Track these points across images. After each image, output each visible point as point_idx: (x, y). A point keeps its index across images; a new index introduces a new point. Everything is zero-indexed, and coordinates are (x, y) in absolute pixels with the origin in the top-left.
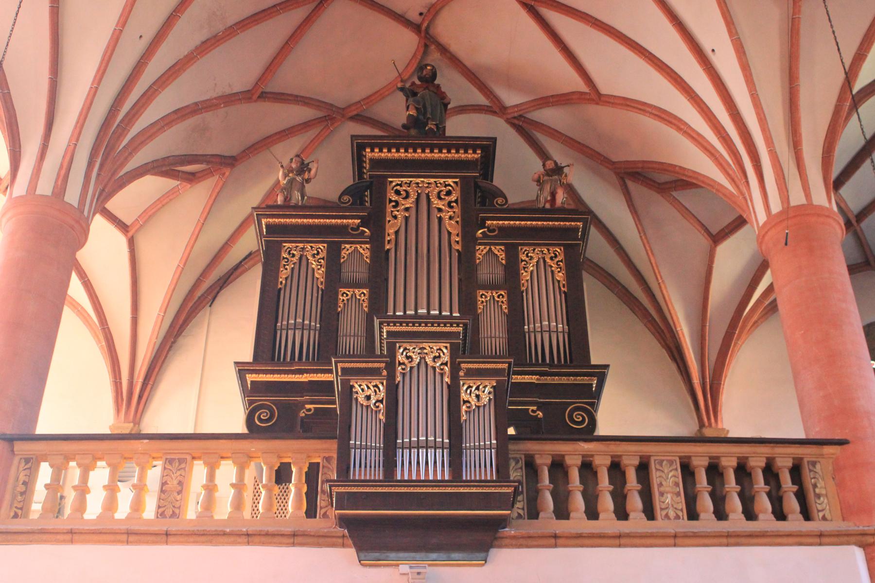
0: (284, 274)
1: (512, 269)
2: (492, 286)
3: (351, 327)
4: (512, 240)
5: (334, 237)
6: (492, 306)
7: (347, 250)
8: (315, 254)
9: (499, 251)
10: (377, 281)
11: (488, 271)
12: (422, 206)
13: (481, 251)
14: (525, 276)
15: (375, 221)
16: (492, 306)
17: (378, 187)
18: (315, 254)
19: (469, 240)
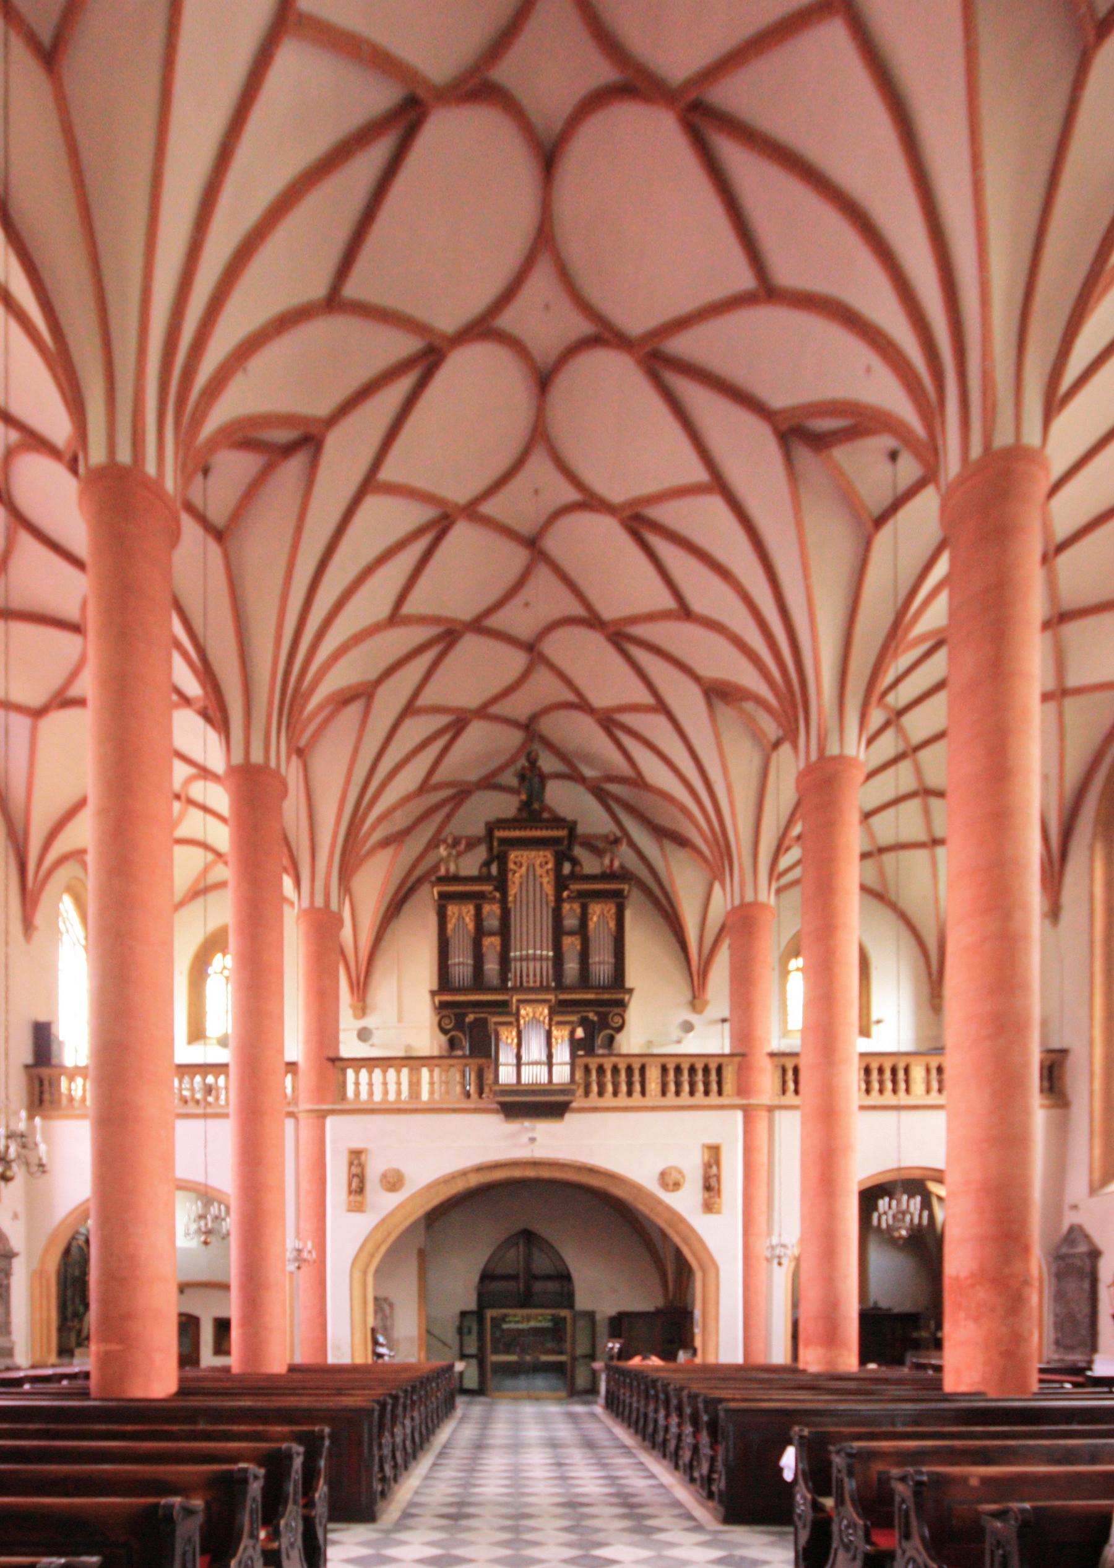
0: (450, 926)
1: (584, 919)
2: (571, 933)
3: (491, 966)
4: (586, 898)
5: (478, 898)
6: (572, 945)
7: (487, 908)
8: (468, 911)
9: (576, 907)
10: (504, 931)
11: (570, 922)
12: (532, 870)
13: (566, 907)
14: (591, 925)
15: (502, 885)
16: (572, 945)
17: (502, 860)
18: (468, 911)
19: (559, 900)
